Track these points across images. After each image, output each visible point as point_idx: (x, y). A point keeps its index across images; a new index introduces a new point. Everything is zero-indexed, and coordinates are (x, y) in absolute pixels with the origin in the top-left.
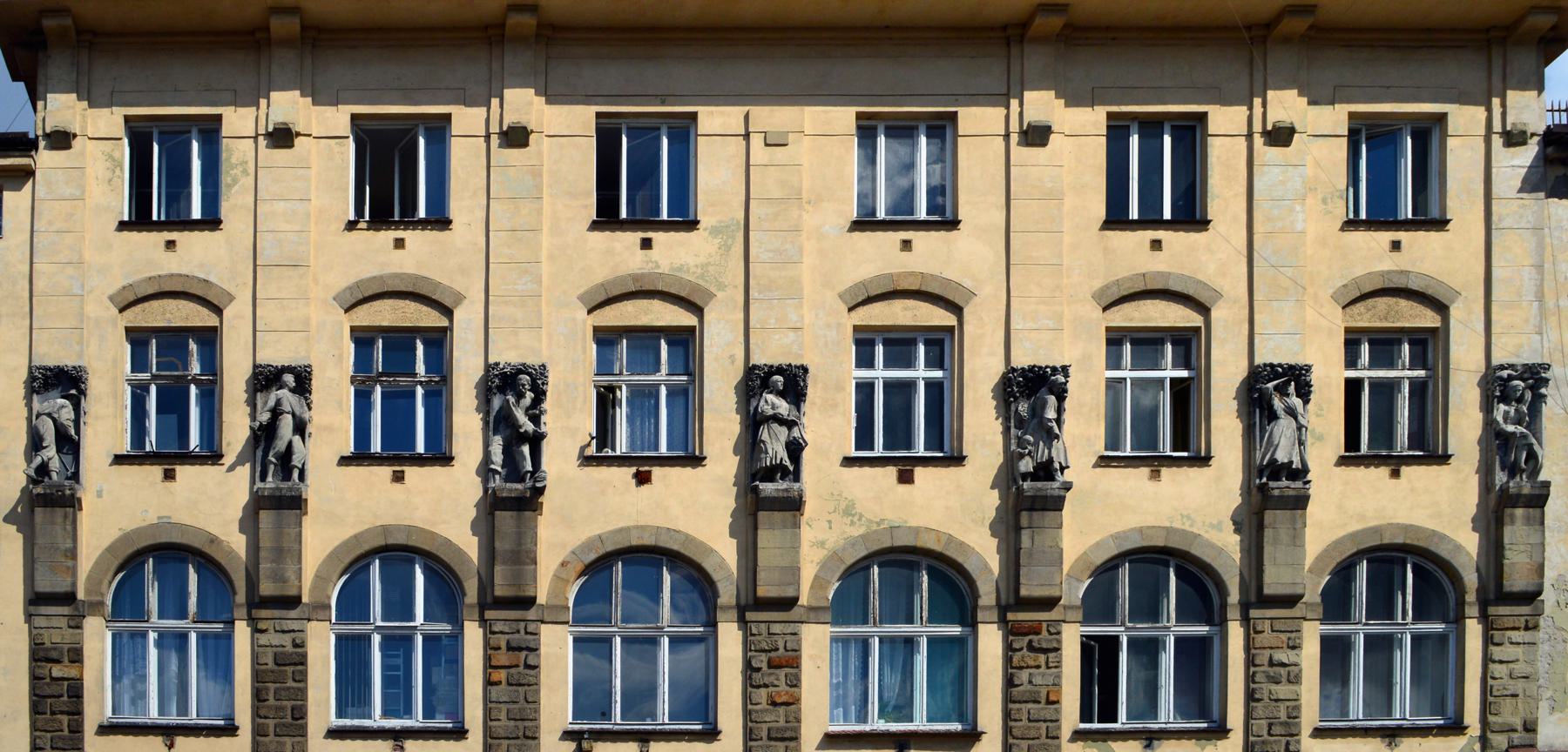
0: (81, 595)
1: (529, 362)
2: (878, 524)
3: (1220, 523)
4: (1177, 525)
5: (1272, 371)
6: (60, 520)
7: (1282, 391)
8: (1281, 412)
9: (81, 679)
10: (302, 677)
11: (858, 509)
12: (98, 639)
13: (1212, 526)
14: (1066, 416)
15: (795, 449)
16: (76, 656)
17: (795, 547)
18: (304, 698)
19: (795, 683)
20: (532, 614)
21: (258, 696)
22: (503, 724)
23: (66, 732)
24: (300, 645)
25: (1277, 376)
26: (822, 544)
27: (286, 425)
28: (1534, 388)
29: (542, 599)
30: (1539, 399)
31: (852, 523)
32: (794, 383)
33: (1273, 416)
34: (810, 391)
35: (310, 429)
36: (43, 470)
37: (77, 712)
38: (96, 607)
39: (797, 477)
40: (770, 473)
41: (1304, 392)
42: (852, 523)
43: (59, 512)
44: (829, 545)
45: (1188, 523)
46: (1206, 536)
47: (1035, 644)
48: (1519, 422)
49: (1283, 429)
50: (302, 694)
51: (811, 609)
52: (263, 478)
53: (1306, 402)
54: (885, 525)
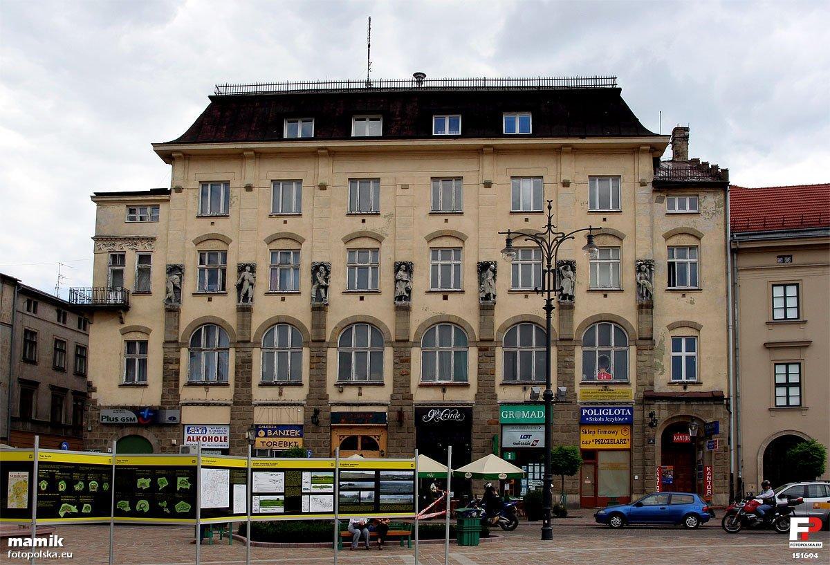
0: (180, 341)
1: (325, 261)
4: (534, 314)
5: (562, 263)
8: (565, 277)
10: (251, 367)
12: (184, 354)
14: (497, 278)
15: (409, 291)
16: (178, 361)
17: (408, 322)
18: (251, 374)
19: (409, 368)
20: (324, 345)
21: (236, 373)
22: (315, 383)
25: (564, 264)
27: (246, 286)
28: (650, 268)
29: (328, 340)
30: (651, 271)
32: (408, 268)
33: (563, 278)
34: (414, 269)
35: (256, 284)
36: (169, 299)
37: (177, 380)
38: (184, 344)
39: (409, 300)
40: (400, 298)
41: (573, 269)
43: (173, 314)
48: (646, 279)
49: (566, 284)
50: (250, 373)
52: (239, 302)
53: (574, 272)
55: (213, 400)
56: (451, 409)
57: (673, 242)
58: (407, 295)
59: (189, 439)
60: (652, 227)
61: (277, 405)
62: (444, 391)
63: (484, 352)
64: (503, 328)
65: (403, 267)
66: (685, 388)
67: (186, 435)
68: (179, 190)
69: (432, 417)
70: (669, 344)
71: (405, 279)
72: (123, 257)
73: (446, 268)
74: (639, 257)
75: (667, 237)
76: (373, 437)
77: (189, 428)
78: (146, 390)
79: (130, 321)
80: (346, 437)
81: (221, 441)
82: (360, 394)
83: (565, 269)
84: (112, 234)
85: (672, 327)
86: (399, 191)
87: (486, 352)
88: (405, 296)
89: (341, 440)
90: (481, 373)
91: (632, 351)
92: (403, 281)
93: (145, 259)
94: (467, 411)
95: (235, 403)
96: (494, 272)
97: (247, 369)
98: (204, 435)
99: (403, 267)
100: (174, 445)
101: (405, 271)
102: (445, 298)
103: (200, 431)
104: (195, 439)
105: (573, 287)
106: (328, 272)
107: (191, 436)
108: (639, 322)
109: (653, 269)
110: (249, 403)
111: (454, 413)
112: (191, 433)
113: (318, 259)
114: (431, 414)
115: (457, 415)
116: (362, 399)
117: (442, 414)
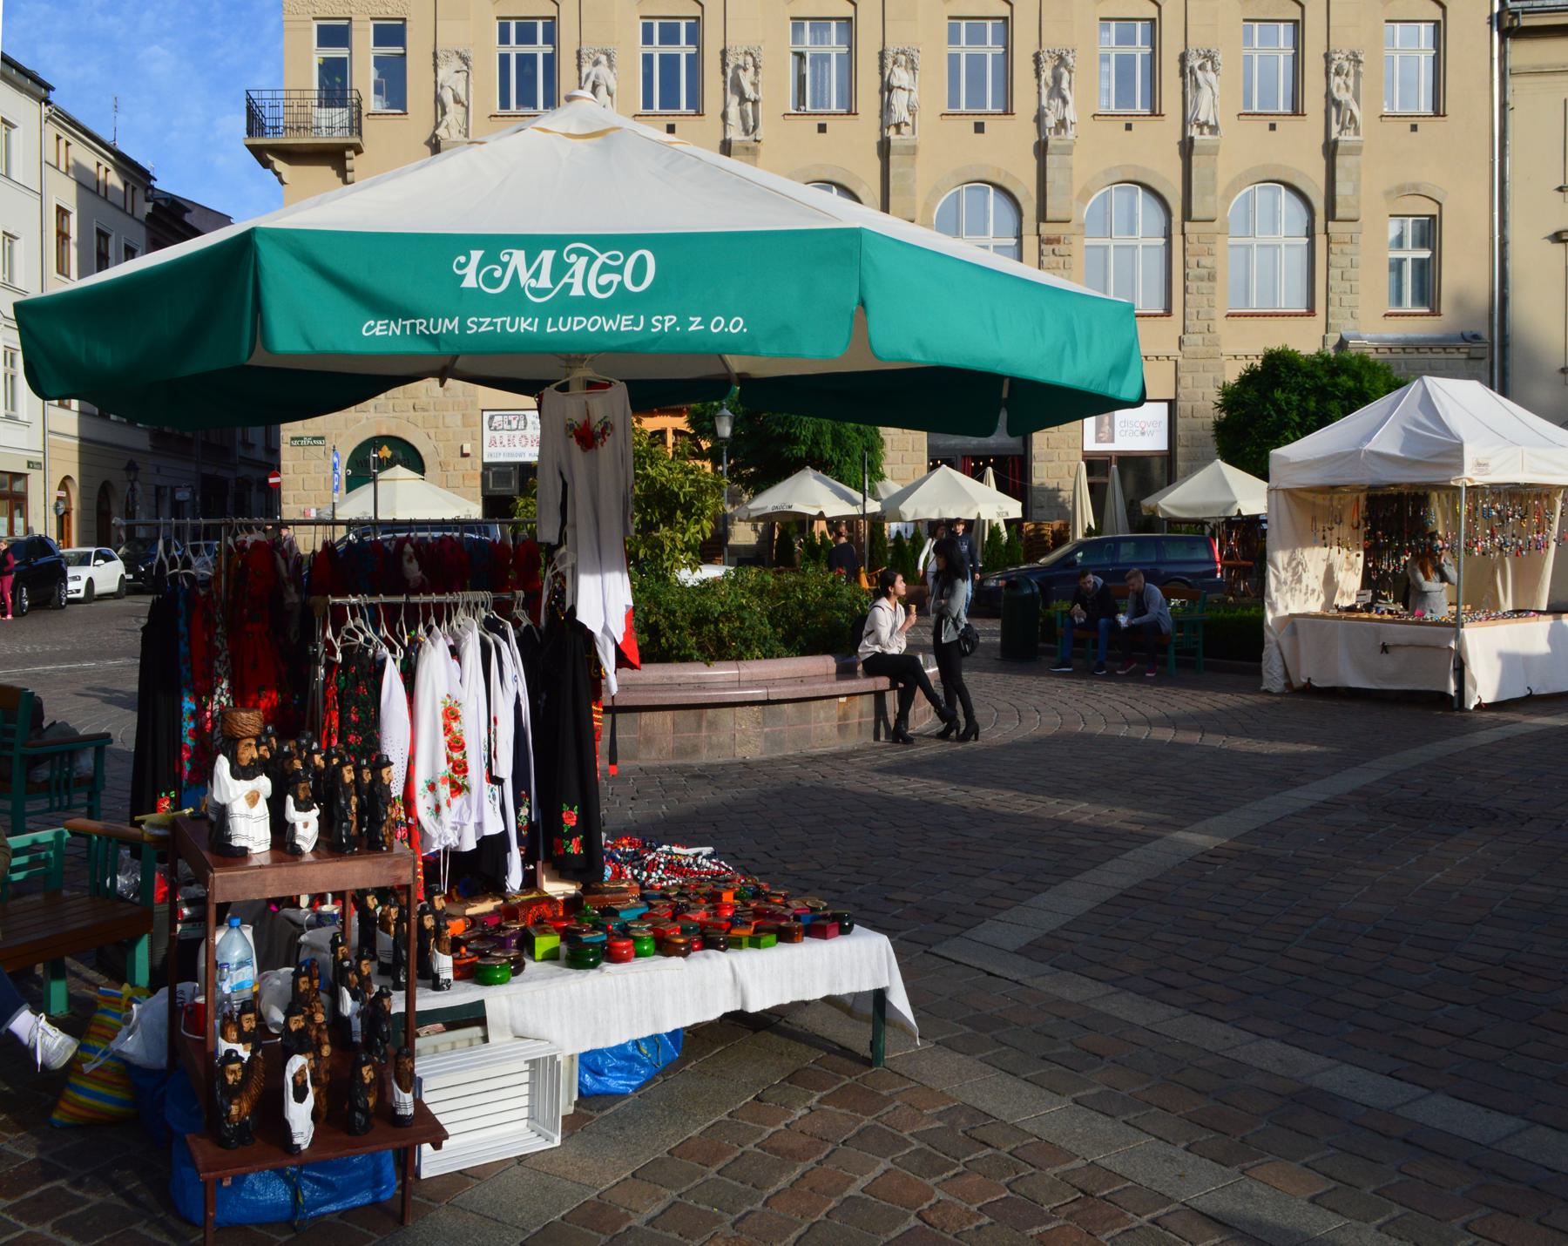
23: (169, 573)
30: (1357, 74)
47: (1056, 252)
59: (493, 443)
63: (1051, 247)
65: (902, 58)
67: (487, 434)
71: (907, 88)
77: (492, 418)
83: (1201, 67)
87: (1056, 247)
88: (907, 124)
92: (904, 89)
98: (522, 432)
99: (902, 58)
100: (466, 455)
104: (505, 442)
107: (496, 434)
109: (1361, 69)
112: (495, 429)
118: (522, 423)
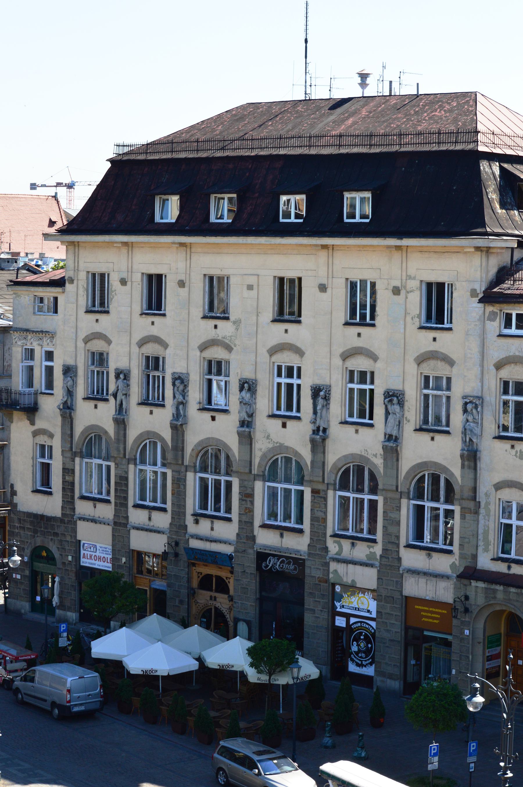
2: (277, 443)
3: (376, 454)
4: (363, 454)
6: (67, 423)
7: (391, 401)
9: (74, 480)
11: (271, 437)
13: (374, 455)
15: (251, 415)
16: (73, 471)
24: (127, 473)
26: (261, 449)
31: (269, 443)
41: (401, 403)
42: (269, 443)
44: (263, 450)
45: (366, 453)
46: (372, 459)
51: (258, 475)
54: (278, 445)
55: (99, 517)
56: (287, 558)
57: (506, 373)
58: (250, 420)
60: (483, 354)
61: (147, 530)
62: (282, 536)
64: (336, 468)
66: (509, 568)
68: (72, 281)
69: (270, 565)
70: (495, 509)
72: (32, 351)
73: (290, 387)
74: (468, 391)
75: (499, 366)
76: (225, 579)
78: (50, 497)
79: (40, 424)
80: (203, 575)
81: (107, 562)
82: (212, 529)
84: (25, 327)
85: (498, 487)
86: (246, 293)
89: (199, 577)
90: (313, 519)
91: (456, 509)
93: (49, 356)
94: (299, 563)
95: (115, 523)
96: (327, 398)
97: (123, 488)
101: (249, 389)
102: (284, 425)
103: (92, 548)
105: (399, 424)
106: (186, 386)
107: (86, 552)
108: (462, 477)
110: (125, 525)
111: (289, 563)
112: (85, 550)
113: (179, 370)
114: (270, 561)
115: (292, 567)
116: (215, 534)
117: (278, 563)
118: (95, 549)
